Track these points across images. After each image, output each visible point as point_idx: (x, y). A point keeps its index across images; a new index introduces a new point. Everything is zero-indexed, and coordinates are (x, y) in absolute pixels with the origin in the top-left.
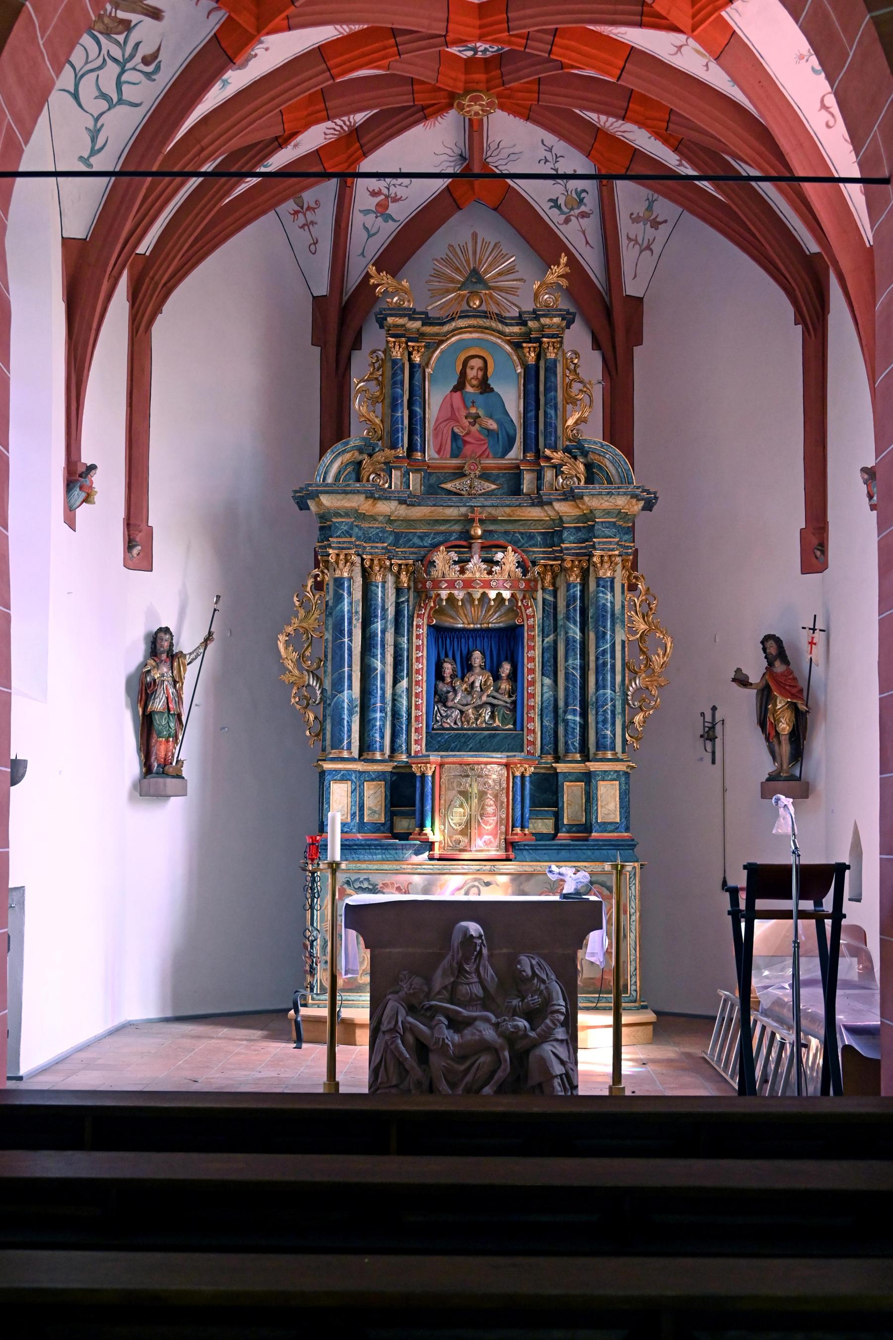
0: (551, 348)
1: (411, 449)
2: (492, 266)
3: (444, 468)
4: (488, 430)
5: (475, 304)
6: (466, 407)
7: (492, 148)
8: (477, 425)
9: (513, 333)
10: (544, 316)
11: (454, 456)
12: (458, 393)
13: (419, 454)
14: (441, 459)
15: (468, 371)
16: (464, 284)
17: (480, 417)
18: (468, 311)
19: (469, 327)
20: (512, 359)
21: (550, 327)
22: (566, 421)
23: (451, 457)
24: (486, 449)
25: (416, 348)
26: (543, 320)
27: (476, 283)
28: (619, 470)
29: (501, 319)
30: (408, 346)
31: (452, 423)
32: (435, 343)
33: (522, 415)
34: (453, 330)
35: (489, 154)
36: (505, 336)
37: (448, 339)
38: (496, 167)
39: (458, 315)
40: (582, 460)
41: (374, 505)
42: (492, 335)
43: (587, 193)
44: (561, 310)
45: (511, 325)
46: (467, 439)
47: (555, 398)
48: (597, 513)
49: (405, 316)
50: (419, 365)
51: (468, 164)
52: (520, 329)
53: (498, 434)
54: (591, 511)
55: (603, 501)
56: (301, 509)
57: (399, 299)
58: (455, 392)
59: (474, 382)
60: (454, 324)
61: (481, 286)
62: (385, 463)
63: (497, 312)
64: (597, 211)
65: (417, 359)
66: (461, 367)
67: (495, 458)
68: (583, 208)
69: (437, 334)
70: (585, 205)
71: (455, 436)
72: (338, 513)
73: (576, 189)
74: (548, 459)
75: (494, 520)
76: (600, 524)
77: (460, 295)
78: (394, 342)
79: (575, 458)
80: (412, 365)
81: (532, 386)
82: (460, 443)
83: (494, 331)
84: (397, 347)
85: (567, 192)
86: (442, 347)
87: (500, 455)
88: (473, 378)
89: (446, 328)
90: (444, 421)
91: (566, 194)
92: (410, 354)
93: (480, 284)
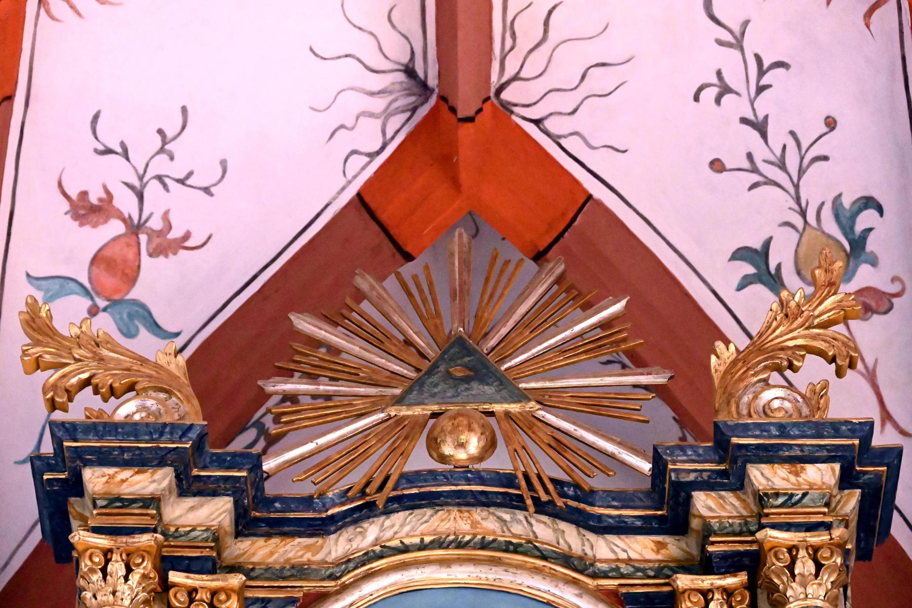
0: (805, 566)
5: (462, 445)
7: (524, 44)
9: (628, 561)
16: (418, 384)
18: (432, 475)
19: (439, 544)
21: (790, 501)
25: (203, 595)
27: (467, 380)
30: (166, 586)
34: (369, 557)
35: (509, 73)
36: (594, 576)
37: (345, 588)
38: (537, 122)
39: (388, 492)
42: (536, 570)
43: (880, 210)
44: (836, 428)
45: (621, 528)
49: (162, 463)
51: (443, 98)
52: (660, 546)
61: (489, 390)
63: (562, 476)
68: (865, 277)
69: (300, 571)
70: (874, 262)
77: (400, 421)
78: (107, 554)
83: (544, 558)
84: (117, 568)
85: (803, 213)
91: (798, 221)
93: (482, 381)
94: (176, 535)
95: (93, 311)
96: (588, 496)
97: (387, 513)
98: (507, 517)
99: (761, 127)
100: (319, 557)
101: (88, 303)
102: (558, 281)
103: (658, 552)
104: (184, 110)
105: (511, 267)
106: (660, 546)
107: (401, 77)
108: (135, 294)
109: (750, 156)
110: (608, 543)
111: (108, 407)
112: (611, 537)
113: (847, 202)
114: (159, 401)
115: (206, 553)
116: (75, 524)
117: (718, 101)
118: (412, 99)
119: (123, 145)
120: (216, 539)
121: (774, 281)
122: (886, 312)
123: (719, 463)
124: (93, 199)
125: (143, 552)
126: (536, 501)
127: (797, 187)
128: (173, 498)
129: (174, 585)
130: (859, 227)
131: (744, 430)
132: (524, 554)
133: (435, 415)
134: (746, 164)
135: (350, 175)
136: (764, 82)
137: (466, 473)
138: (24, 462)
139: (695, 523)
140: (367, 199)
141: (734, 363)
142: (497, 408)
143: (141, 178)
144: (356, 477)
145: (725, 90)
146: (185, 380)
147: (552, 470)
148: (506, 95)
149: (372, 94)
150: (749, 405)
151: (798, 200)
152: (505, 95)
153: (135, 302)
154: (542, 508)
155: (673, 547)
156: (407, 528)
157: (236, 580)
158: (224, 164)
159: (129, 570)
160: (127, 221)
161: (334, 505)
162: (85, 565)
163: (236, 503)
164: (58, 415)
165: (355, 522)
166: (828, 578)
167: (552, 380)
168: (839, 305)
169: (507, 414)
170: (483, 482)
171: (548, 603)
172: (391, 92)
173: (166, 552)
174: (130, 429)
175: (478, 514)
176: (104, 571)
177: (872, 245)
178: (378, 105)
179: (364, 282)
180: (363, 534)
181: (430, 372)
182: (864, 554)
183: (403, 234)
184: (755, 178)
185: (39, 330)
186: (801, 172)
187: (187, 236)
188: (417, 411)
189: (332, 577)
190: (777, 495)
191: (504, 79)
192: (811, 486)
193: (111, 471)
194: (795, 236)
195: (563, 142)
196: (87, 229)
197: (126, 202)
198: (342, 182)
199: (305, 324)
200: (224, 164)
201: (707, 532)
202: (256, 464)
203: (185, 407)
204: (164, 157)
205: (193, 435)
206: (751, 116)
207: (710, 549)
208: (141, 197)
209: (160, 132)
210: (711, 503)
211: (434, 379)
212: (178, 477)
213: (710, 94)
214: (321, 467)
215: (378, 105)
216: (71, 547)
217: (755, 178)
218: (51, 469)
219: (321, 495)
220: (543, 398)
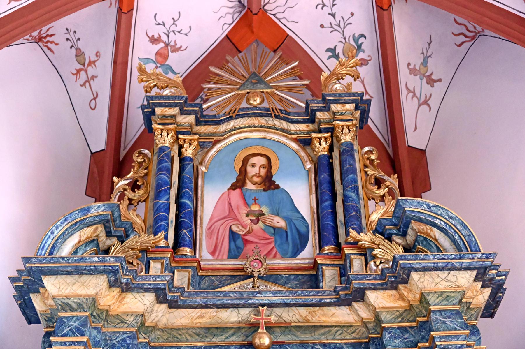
0: (346, 131)
1: (178, 244)
2: (274, 69)
3: (218, 270)
4: (274, 228)
6: (247, 204)
8: (260, 223)
9: (299, 130)
10: (336, 102)
11: (232, 256)
12: (238, 191)
13: (188, 250)
14: (217, 259)
15: (249, 168)
16: (243, 84)
17: (264, 215)
18: (248, 109)
19: (249, 127)
20: (299, 157)
21: (342, 114)
22: (369, 216)
23: (228, 258)
24: (273, 248)
26: (334, 107)
27: (256, 83)
28: (457, 237)
29: (285, 116)
30: (178, 138)
31: (230, 222)
32: (211, 142)
33: (315, 211)
34: (231, 130)
36: (290, 134)
37: (225, 139)
38: (274, 15)
39: (236, 113)
40: (399, 241)
41: (121, 300)
42: (275, 133)
43: (365, 37)
44: (354, 94)
45: (298, 122)
46: (247, 238)
47: (355, 181)
48: (432, 299)
49: (176, 106)
50: (191, 160)
51: (249, 9)
52: (308, 126)
53: (286, 232)
54: (422, 294)
55: (439, 280)
56: (30, 322)
57: (170, 92)
58: (234, 190)
59: (256, 179)
60: (232, 124)
61: (262, 86)
62: (142, 251)
63: (282, 108)
64: (375, 57)
65: (189, 151)
66: (240, 165)
67: (283, 257)
68: (361, 55)
69: (213, 134)
70: (364, 51)
71: (233, 235)
72: (68, 304)
73: (354, 35)
74: (355, 244)
75: (286, 327)
76: (438, 313)
78: (162, 130)
79: (389, 239)
80: (182, 160)
81: (325, 176)
82: (239, 242)
83: (277, 130)
84: (165, 134)
85: (345, 39)
86: (219, 146)
87: (289, 255)
88: (254, 176)
89: (223, 128)
90: (219, 220)
91: (343, 41)
92: (181, 147)
93: (261, 84)
94: (180, 125)
95: (157, 67)
96: (289, 113)
97: (236, 119)
98: (267, 119)
99: (334, 16)
100: (218, 130)
101: (154, 65)
102: (280, 57)
103: (307, 128)
104: (179, 13)
105: (267, 54)
106: (308, 126)
107: (237, 3)
108: (168, 62)
109: (331, 23)
110: (294, 126)
111: (161, 92)
112: (295, 124)
113: (356, 35)
114: (174, 90)
115: (188, 130)
116: (153, 122)
117: (322, 8)
118: (241, 9)
119: (163, 22)
120: (191, 126)
121: (337, 57)
122: (367, 65)
123: (324, 104)
124: (156, 37)
125: (171, 130)
126: (275, 115)
127: (343, 32)
128: (179, 116)
129: (180, 138)
130: (360, 42)
131: (330, 95)
132: (272, 129)
133: (248, 93)
134: (330, 26)
135: (224, 30)
136: (334, 3)
137: (256, 108)
138: (139, 108)
139: (317, 120)
140: (229, 36)
141: (327, 78)
142: (264, 91)
143: (168, 31)
144: (227, 110)
145: (324, 5)
146: (181, 84)
147: (279, 107)
148: (266, 8)
149: (230, 8)
150: (331, 89)
151: (343, 35)
152: (266, 8)
153: (168, 65)
154: (276, 117)
155: (311, 126)
156: (241, 123)
157: (196, 137)
158: (190, 27)
159: (168, 134)
160: (165, 43)
161: (222, 117)
162: (156, 133)
163: (196, 117)
164: (148, 94)
165: (227, 121)
166: (352, 134)
167: (279, 83)
168: (355, 62)
169: (267, 92)
170: (261, 110)
171: (278, 142)
172: (235, 7)
173: (177, 129)
174: (167, 97)
175: (260, 118)
176: (161, 135)
177: (363, 47)
178: (231, 11)
179: (228, 58)
180: (230, 124)
181: (246, 81)
182: (361, 128)
183: (238, 46)
184: (332, 29)
185: (142, 72)
186: (344, 27)
187: (181, 47)
188: (243, 92)
189: (221, 136)
190: (338, 112)
191: (265, 3)
192: (348, 110)
193: (162, 108)
194: (343, 45)
195: (281, 20)
196: (154, 45)
197: (164, 38)
198: (222, 32)
199: (213, 69)
200: (190, 27)
201: (320, 122)
202: (201, 107)
203: (182, 91)
204: (174, 25)
205: (184, 99)
206: (331, 13)
207: (321, 127)
208: (168, 36)
209: (173, 19)
210: (321, 115)
211: (247, 83)
212: (180, 110)
213: (320, 7)
214: (218, 107)
215: (231, 11)
216: (152, 129)
217: (332, 29)
218: (147, 108)
219: (218, 114)
220: (277, 88)
